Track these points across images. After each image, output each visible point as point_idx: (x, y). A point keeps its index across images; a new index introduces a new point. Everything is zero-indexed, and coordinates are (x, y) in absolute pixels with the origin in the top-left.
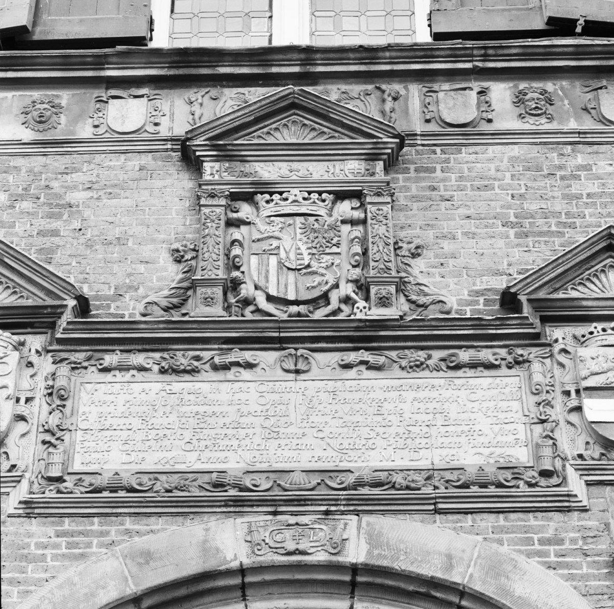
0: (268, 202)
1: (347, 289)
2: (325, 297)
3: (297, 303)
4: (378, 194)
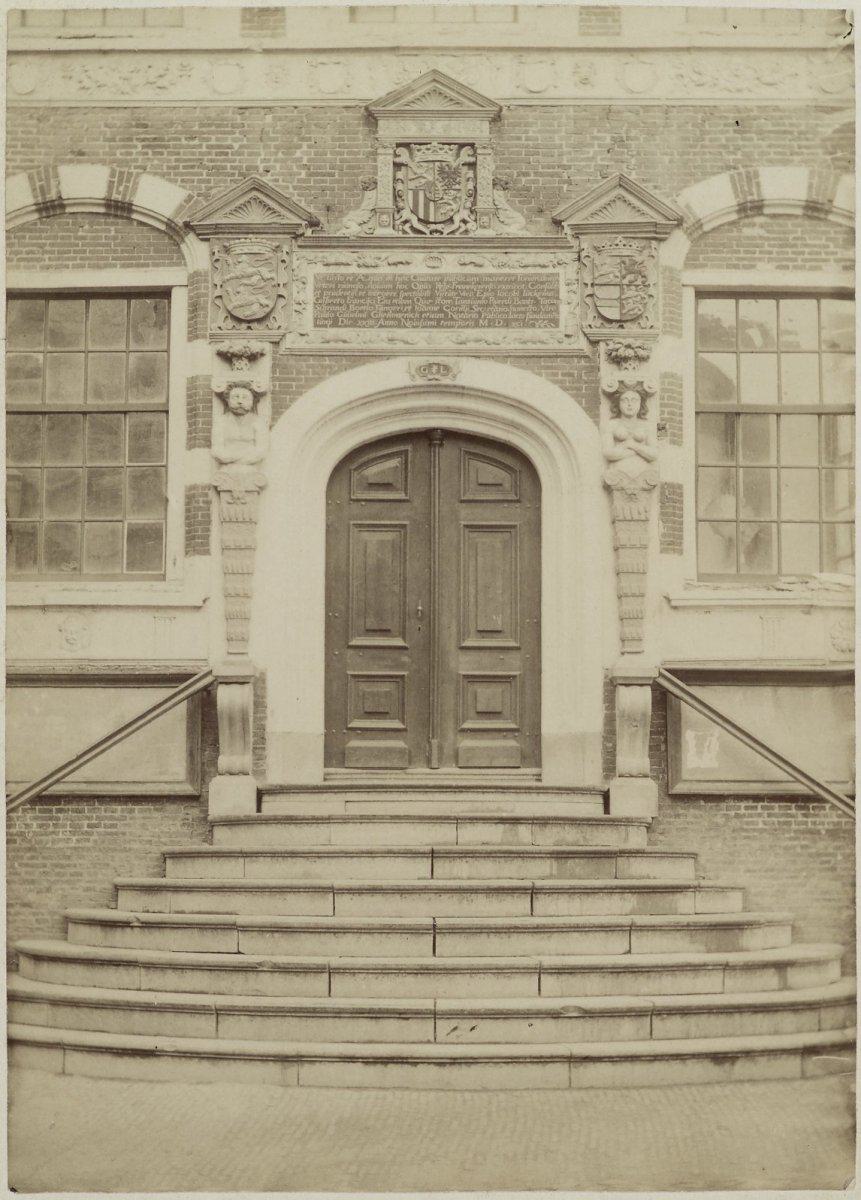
0: (418, 150)
1: (465, 214)
2: (451, 220)
3: (435, 223)
4: (484, 148)
